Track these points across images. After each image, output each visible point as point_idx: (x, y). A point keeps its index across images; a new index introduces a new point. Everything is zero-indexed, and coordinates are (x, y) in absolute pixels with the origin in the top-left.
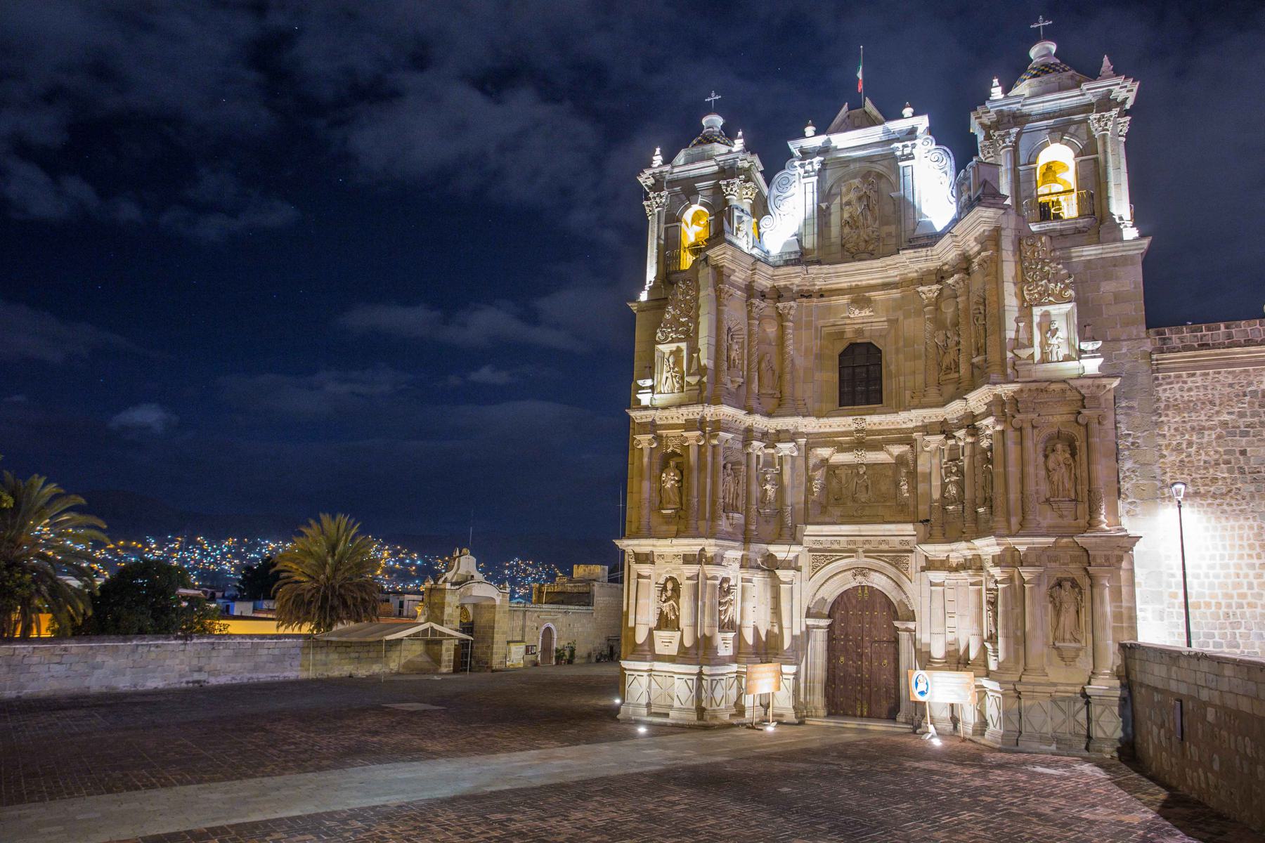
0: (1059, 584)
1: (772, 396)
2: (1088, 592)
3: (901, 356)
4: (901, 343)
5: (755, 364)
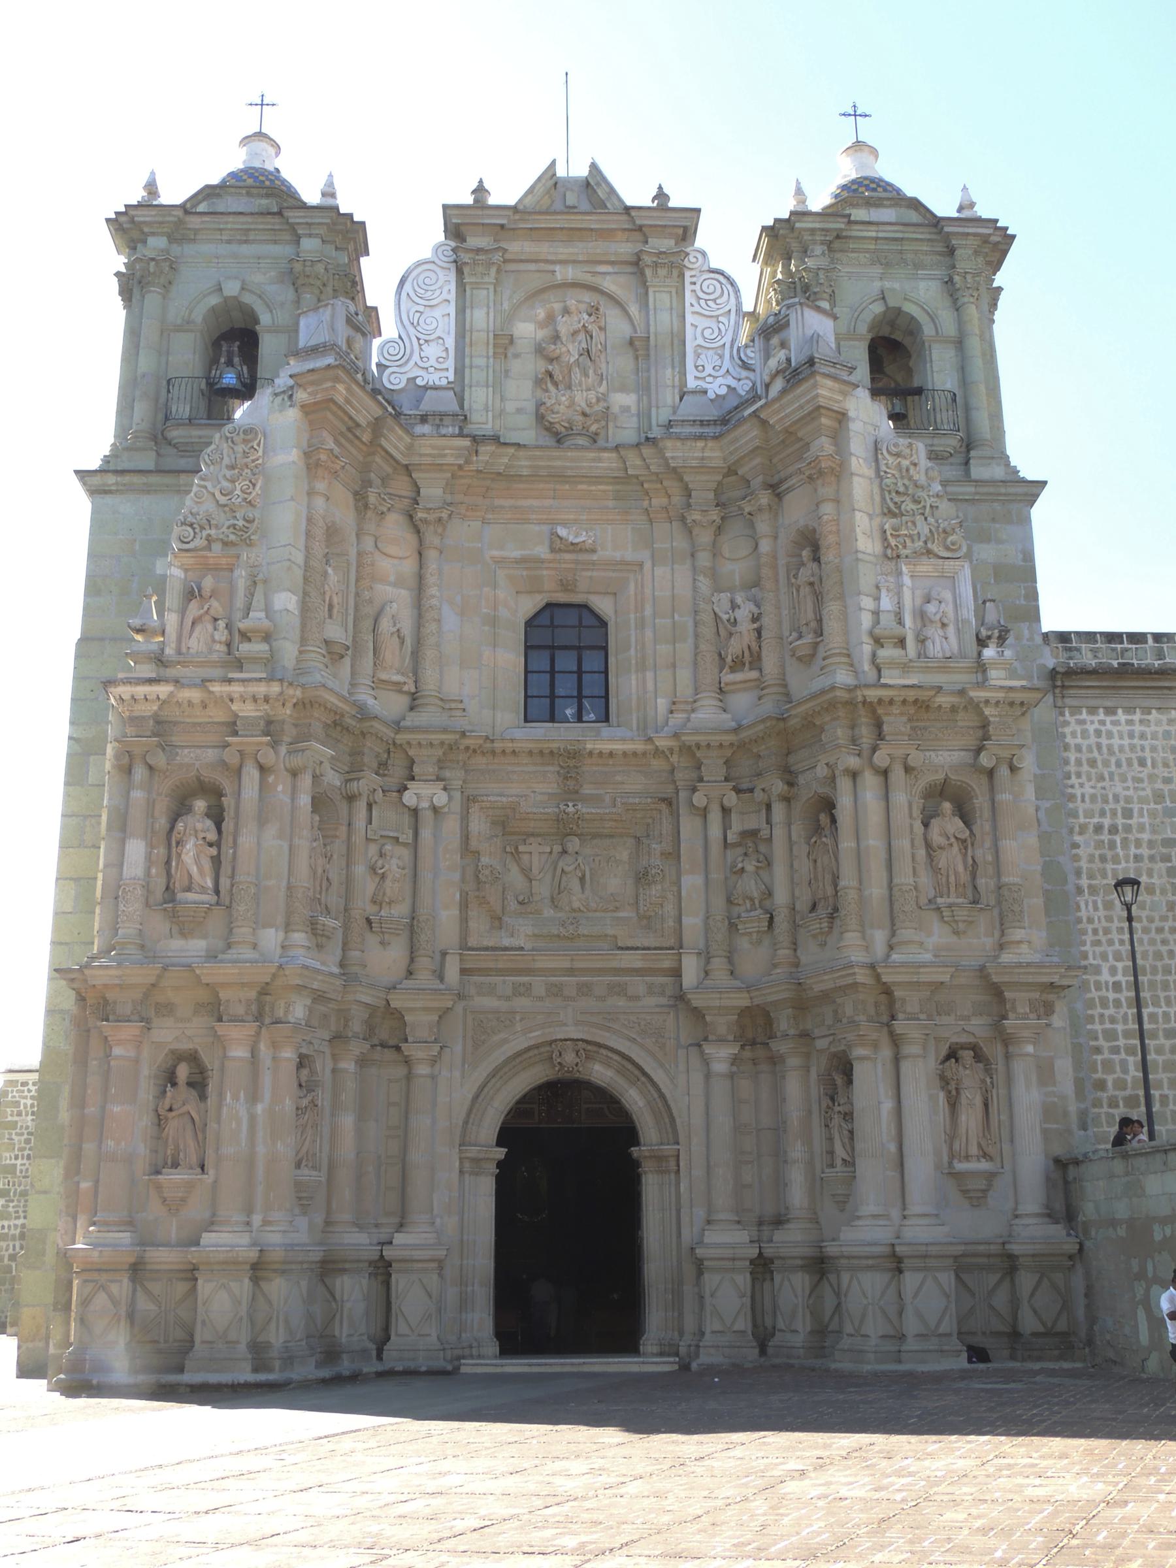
0: (953, 1054)
1: (398, 687)
2: (1001, 1067)
3: (649, 634)
4: (648, 611)
5: (368, 624)
